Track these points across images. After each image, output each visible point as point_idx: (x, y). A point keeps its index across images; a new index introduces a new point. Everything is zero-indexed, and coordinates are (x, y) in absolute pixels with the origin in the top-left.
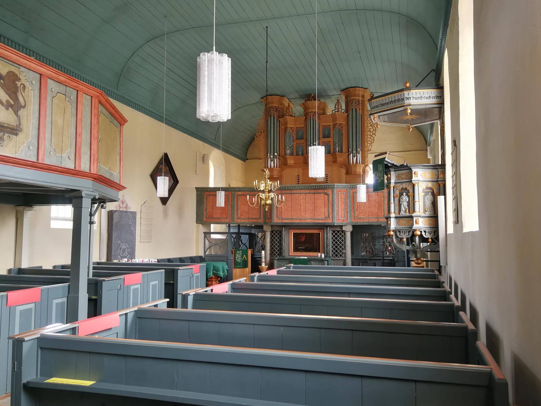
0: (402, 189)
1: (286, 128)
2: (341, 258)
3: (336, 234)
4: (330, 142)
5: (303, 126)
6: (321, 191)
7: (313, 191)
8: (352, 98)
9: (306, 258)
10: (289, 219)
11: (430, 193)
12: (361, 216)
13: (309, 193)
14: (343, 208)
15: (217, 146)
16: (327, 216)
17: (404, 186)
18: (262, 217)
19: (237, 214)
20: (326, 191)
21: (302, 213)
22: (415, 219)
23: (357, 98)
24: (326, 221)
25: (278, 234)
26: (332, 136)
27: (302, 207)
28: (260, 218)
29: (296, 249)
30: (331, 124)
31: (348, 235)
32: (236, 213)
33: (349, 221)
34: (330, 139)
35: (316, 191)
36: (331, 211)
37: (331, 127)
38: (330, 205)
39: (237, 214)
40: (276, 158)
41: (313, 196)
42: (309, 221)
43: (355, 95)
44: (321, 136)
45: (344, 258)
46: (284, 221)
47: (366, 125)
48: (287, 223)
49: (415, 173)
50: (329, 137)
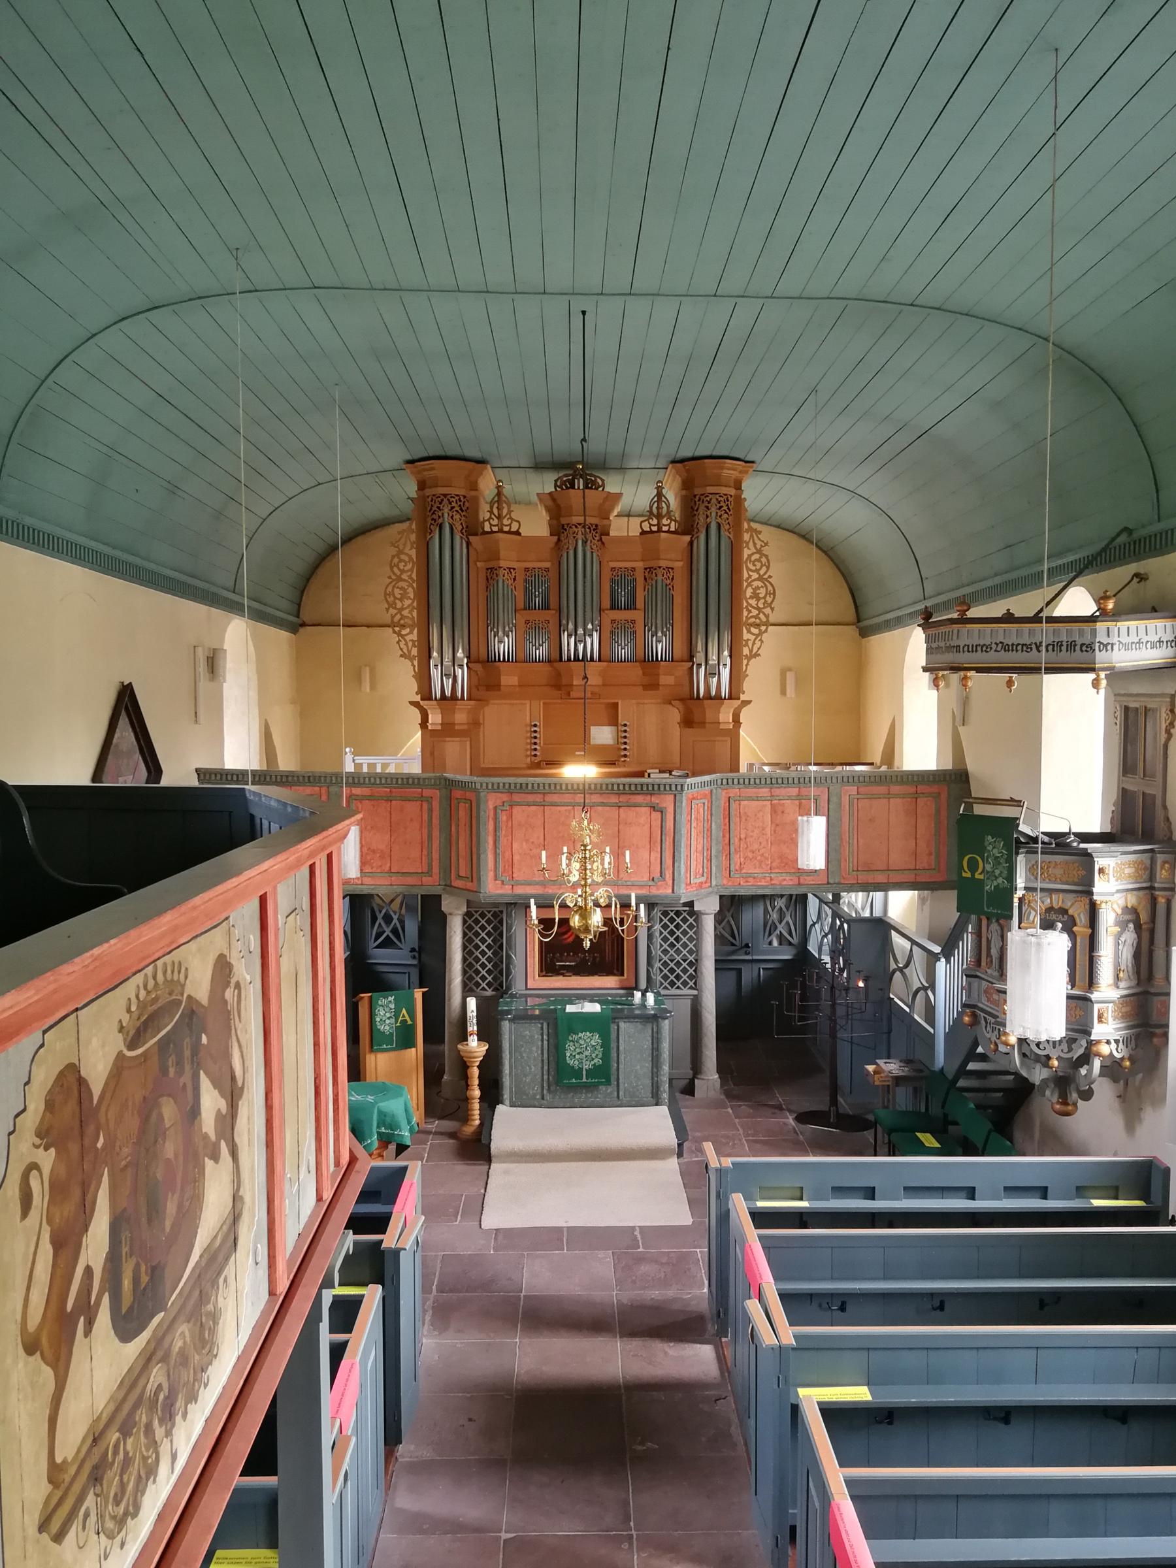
0: (1050, 909)
1: (492, 572)
2: (686, 991)
3: (672, 920)
4: (633, 622)
5: (547, 565)
6: (639, 799)
7: (614, 799)
8: (710, 489)
9: (596, 1008)
10: (537, 884)
11: (1131, 926)
12: (749, 869)
13: (603, 804)
14: (700, 847)
15: (235, 608)
17: (1057, 901)
18: (436, 870)
20: (655, 800)
22: (1096, 1007)
23: (724, 490)
25: (489, 922)
26: (640, 603)
28: (429, 873)
29: (548, 968)
30: (639, 565)
31: (709, 926)
33: (714, 883)
35: (623, 798)
36: (668, 861)
38: (667, 842)
40: (461, 666)
41: (615, 811)
44: (606, 603)
45: (695, 992)
47: (746, 575)
49: (1101, 871)
50: (631, 606)
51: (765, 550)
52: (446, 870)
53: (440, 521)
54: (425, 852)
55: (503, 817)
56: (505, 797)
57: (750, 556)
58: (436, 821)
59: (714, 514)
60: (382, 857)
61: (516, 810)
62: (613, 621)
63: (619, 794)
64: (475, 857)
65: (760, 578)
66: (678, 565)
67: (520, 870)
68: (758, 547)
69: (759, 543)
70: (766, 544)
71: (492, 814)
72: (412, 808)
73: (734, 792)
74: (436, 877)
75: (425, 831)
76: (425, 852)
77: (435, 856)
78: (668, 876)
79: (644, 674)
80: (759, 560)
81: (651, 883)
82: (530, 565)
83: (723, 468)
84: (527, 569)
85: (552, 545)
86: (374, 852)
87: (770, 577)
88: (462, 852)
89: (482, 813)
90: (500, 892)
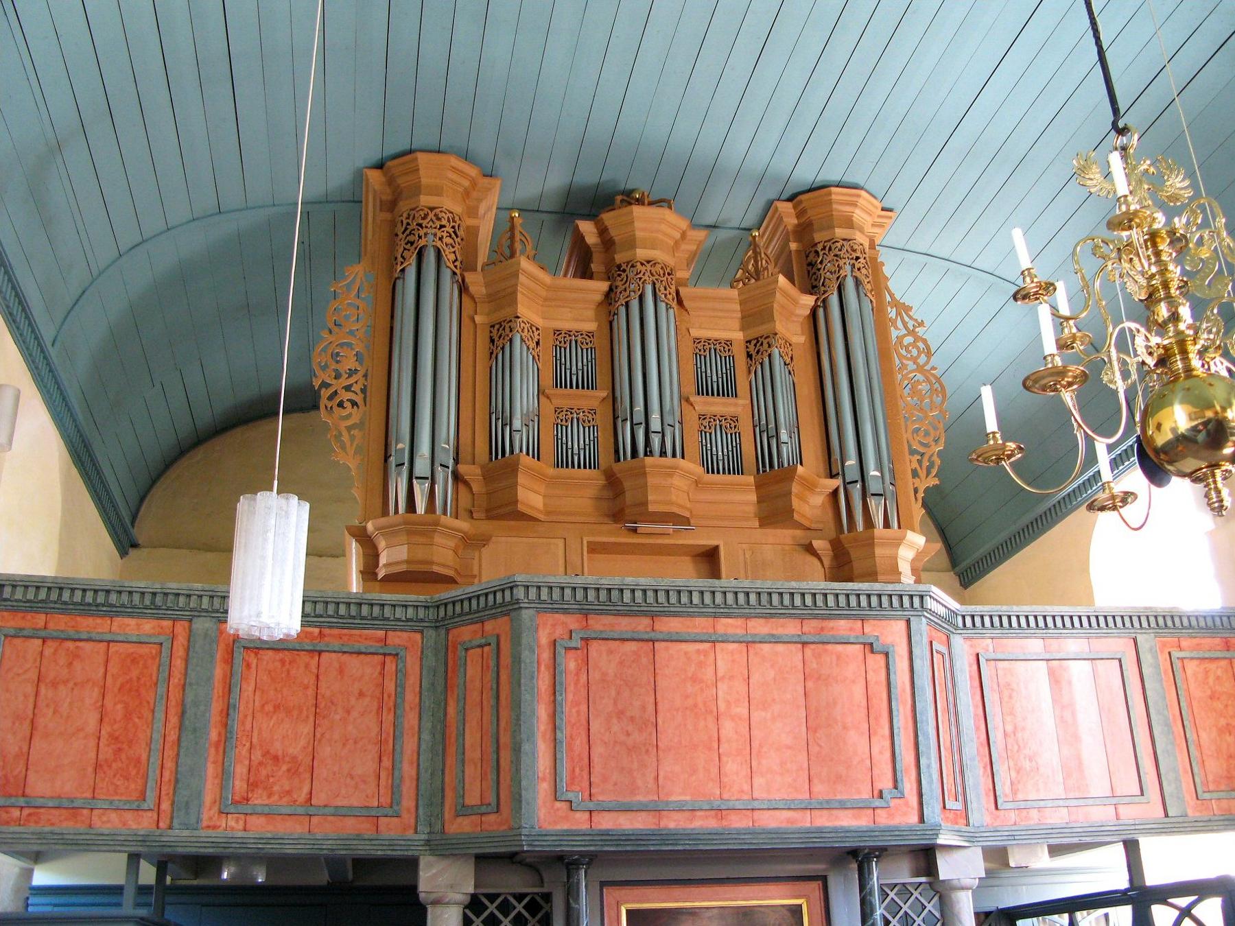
1: (500, 335)
4: (735, 419)
5: (591, 326)
6: (842, 626)
7: (790, 628)
13: (776, 640)
16: (886, 783)
19: (224, 775)
21: (731, 766)
24: (883, 820)
27: (728, 728)
32: (211, 769)
34: (738, 406)
35: (811, 625)
39: (224, 775)
42: (772, 821)
43: (849, 223)
46: (606, 822)
48: (626, 837)
50: (728, 390)
51: (920, 331)
52: (433, 797)
53: (422, 243)
54: (387, 762)
55: (570, 663)
56: (572, 622)
57: (900, 339)
58: (411, 697)
59: (848, 268)
60: (293, 772)
61: (594, 647)
62: (702, 417)
63: (802, 618)
64: (505, 756)
65: (920, 369)
67: (605, 779)
69: (910, 324)
70: (921, 324)
71: (546, 655)
72: (363, 670)
73: (986, 646)
74: (408, 818)
75: (388, 718)
76: (387, 762)
77: (408, 770)
78: (909, 786)
80: (914, 345)
81: (878, 803)
83: (854, 205)
84: (557, 332)
85: (599, 297)
86: (276, 759)
87: (934, 368)
88: (473, 754)
89: (525, 654)
90: (565, 826)
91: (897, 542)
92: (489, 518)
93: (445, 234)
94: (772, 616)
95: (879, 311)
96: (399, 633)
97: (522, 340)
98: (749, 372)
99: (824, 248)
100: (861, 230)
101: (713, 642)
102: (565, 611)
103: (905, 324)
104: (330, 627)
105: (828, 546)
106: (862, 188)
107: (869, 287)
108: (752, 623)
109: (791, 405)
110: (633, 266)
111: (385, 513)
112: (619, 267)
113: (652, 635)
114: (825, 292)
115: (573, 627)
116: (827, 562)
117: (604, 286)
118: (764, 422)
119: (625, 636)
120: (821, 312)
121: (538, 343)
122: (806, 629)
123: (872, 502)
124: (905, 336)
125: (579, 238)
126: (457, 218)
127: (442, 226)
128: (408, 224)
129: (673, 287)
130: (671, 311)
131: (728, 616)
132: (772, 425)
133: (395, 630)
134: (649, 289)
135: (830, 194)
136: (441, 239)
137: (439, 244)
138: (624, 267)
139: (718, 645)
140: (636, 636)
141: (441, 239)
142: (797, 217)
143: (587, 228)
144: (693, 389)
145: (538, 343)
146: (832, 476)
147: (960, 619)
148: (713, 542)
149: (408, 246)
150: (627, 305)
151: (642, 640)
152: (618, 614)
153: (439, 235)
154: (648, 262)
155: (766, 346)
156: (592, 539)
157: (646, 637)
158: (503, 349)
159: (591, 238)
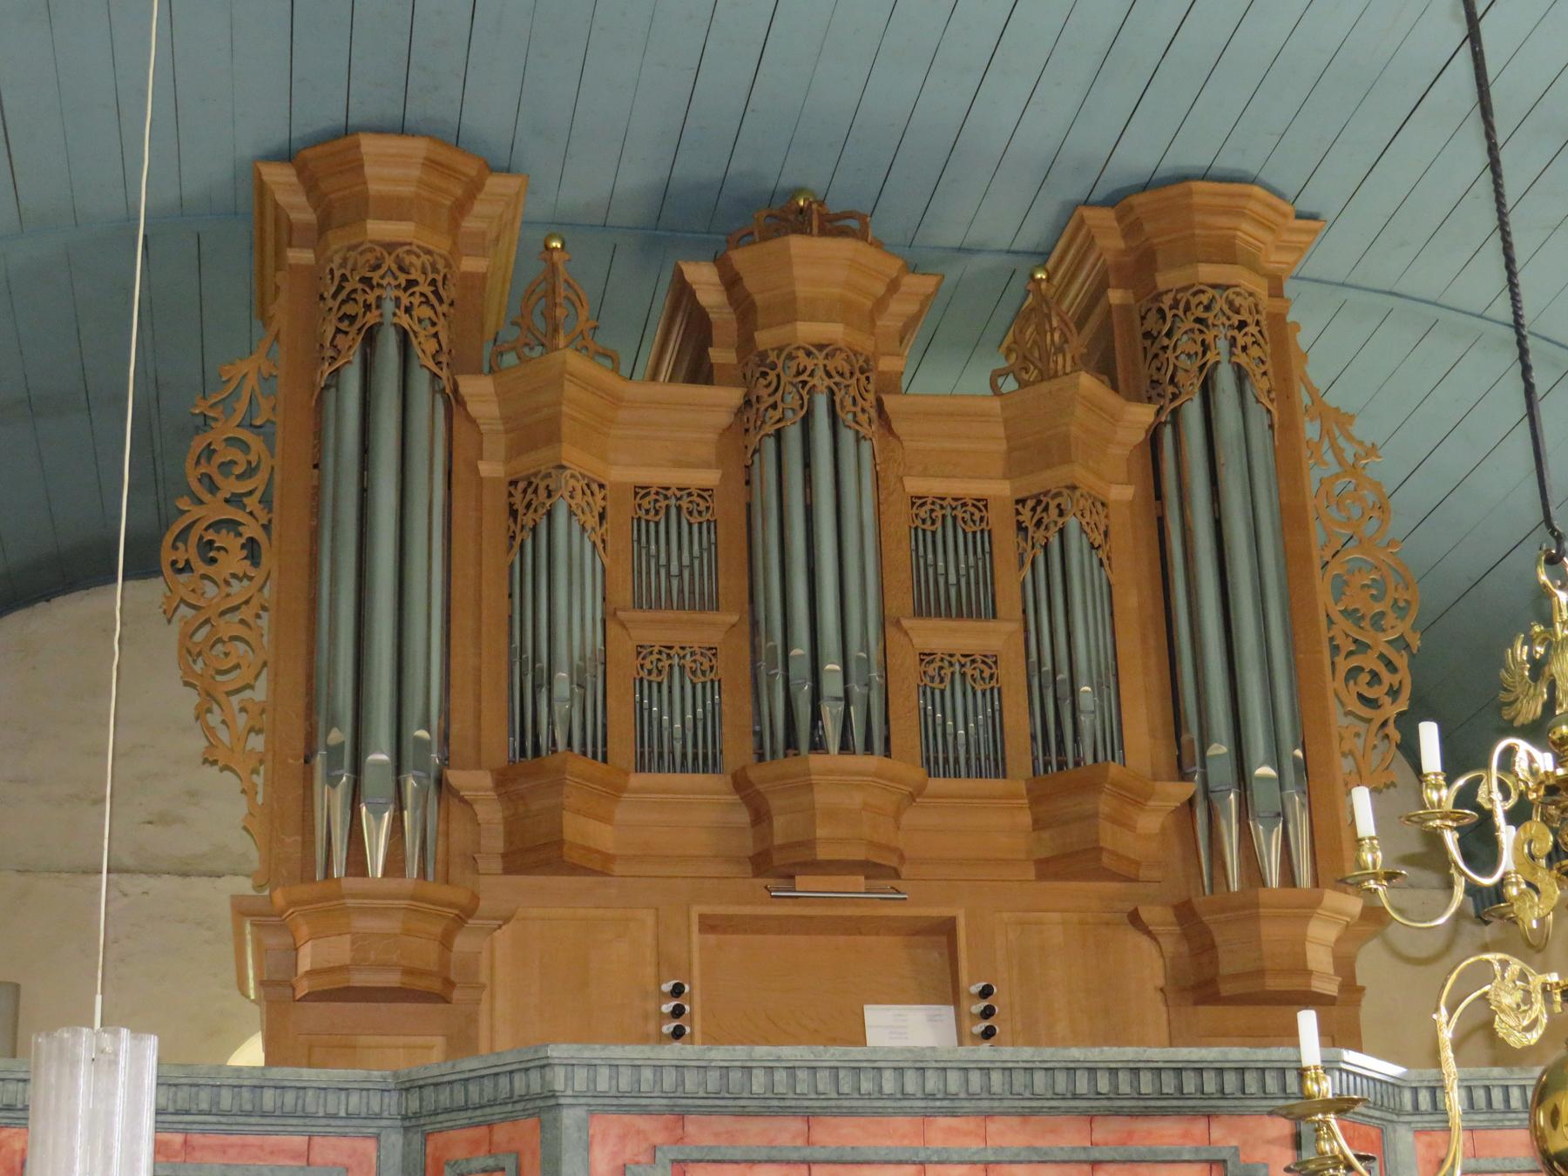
1: (527, 502)
8: (1208, 272)
20: (1223, 1136)
26: (1009, 601)
30: (999, 489)
34: (995, 637)
35: (1107, 1131)
37: (1001, 524)
53: (371, 318)
59: (1223, 345)
66: (1122, 493)
68: (1349, 457)
69: (1349, 453)
70: (1373, 450)
79: (1038, 824)
82: (656, 476)
83: (1238, 212)
85: (724, 418)
91: (1310, 907)
92: (507, 871)
93: (416, 300)
94: (1034, 1112)
95: (1284, 430)
96: (333, 1140)
97: (571, 513)
98: (1022, 564)
99: (1175, 306)
100: (1253, 266)
101: (922, 1163)
102: (645, 1111)
103: (1338, 453)
104: (203, 1132)
105: (1170, 916)
106: (1253, 181)
107: (1264, 384)
108: (994, 1126)
109: (1104, 629)
110: (790, 357)
111: (306, 876)
112: (763, 355)
113: (807, 1153)
114: (1175, 397)
115: (658, 1139)
116: (1169, 945)
117: (735, 396)
118: (1047, 667)
119: (755, 1156)
120: (1168, 432)
121: (602, 516)
122: (1097, 1136)
123: (1258, 829)
124: (1337, 476)
125: (683, 291)
126: (440, 265)
127: (412, 283)
128: (344, 278)
129: (871, 397)
130: (865, 445)
131: (953, 1113)
132: (1063, 675)
133: (325, 1135)
134: (821, 403)
135: (1190, 193)
136: (408, 310)
137: (405, 320)
138: (772, 357)
139: (929, 1168)
140: (775, 1154)
141: (408, 310)
142: (1126, 235)
143: (704, 279)
144: (908, 603)
145: (602, 516)
146: (1184, 776)
147: (1407, 1097)
148: (946, 912)
149: (344, 326)
150: (779, 436)
151: (788, 1162)
152: (743, 1113)
153: (405, 301)
154: (821, 347)
155: (1053, 512)
156: (707, 910)
157: (795, 1156)
158: (534, 530)
159: (710, 294)
